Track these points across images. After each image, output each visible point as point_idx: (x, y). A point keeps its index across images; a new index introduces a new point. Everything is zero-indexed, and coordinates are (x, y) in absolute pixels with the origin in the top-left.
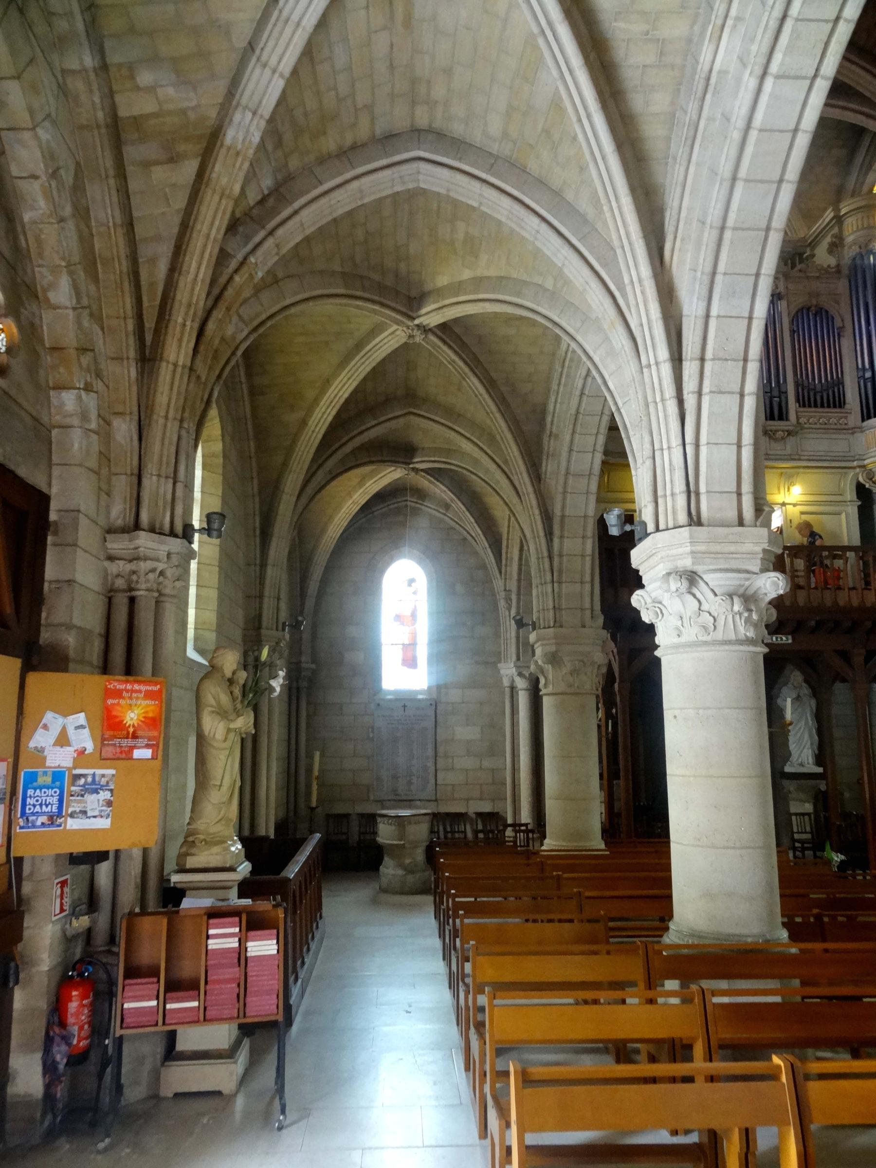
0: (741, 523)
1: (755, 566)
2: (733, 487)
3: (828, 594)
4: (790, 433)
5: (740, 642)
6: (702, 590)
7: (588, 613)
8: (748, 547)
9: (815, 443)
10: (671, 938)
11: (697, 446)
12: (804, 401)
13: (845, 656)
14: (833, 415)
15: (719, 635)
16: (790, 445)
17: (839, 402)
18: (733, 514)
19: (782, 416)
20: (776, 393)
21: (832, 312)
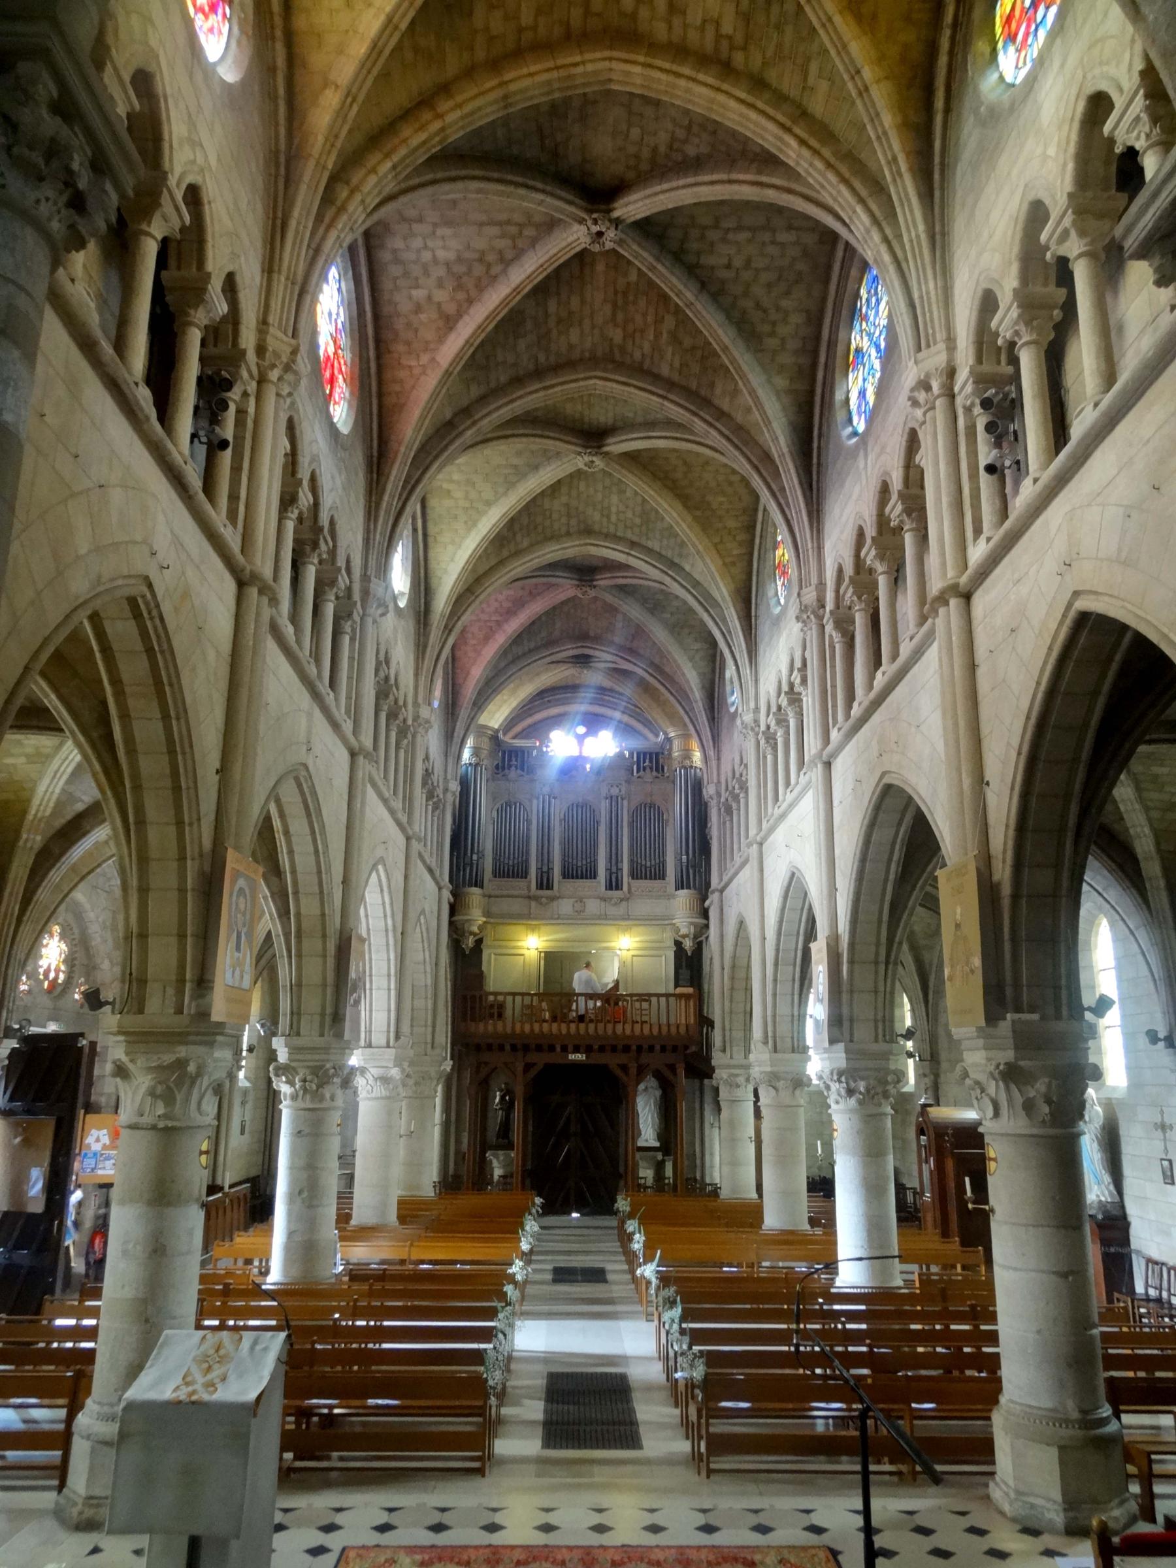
0: (388, 1046)
1: (391, 1065)
2: (385, 1029)
3: (610, 1026)
4: (622, 900)
5: (382, 1098)
6: (368, 1076)
7: (429, 1046)
8: (386, 1057)
9: (642, 906)
10: (353, 1222)
11: (371, 1011)
12: (635, 875)
13: (624, 1068)
14: (657, 884)
15: (373, 1095)
16: (622, 909)
17: (661, 875)
18: (383, 1042)
19: (618, 887)
20: (614, 869)
21: (662, 808)
